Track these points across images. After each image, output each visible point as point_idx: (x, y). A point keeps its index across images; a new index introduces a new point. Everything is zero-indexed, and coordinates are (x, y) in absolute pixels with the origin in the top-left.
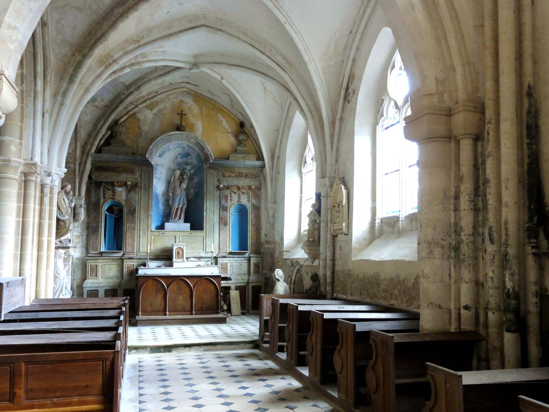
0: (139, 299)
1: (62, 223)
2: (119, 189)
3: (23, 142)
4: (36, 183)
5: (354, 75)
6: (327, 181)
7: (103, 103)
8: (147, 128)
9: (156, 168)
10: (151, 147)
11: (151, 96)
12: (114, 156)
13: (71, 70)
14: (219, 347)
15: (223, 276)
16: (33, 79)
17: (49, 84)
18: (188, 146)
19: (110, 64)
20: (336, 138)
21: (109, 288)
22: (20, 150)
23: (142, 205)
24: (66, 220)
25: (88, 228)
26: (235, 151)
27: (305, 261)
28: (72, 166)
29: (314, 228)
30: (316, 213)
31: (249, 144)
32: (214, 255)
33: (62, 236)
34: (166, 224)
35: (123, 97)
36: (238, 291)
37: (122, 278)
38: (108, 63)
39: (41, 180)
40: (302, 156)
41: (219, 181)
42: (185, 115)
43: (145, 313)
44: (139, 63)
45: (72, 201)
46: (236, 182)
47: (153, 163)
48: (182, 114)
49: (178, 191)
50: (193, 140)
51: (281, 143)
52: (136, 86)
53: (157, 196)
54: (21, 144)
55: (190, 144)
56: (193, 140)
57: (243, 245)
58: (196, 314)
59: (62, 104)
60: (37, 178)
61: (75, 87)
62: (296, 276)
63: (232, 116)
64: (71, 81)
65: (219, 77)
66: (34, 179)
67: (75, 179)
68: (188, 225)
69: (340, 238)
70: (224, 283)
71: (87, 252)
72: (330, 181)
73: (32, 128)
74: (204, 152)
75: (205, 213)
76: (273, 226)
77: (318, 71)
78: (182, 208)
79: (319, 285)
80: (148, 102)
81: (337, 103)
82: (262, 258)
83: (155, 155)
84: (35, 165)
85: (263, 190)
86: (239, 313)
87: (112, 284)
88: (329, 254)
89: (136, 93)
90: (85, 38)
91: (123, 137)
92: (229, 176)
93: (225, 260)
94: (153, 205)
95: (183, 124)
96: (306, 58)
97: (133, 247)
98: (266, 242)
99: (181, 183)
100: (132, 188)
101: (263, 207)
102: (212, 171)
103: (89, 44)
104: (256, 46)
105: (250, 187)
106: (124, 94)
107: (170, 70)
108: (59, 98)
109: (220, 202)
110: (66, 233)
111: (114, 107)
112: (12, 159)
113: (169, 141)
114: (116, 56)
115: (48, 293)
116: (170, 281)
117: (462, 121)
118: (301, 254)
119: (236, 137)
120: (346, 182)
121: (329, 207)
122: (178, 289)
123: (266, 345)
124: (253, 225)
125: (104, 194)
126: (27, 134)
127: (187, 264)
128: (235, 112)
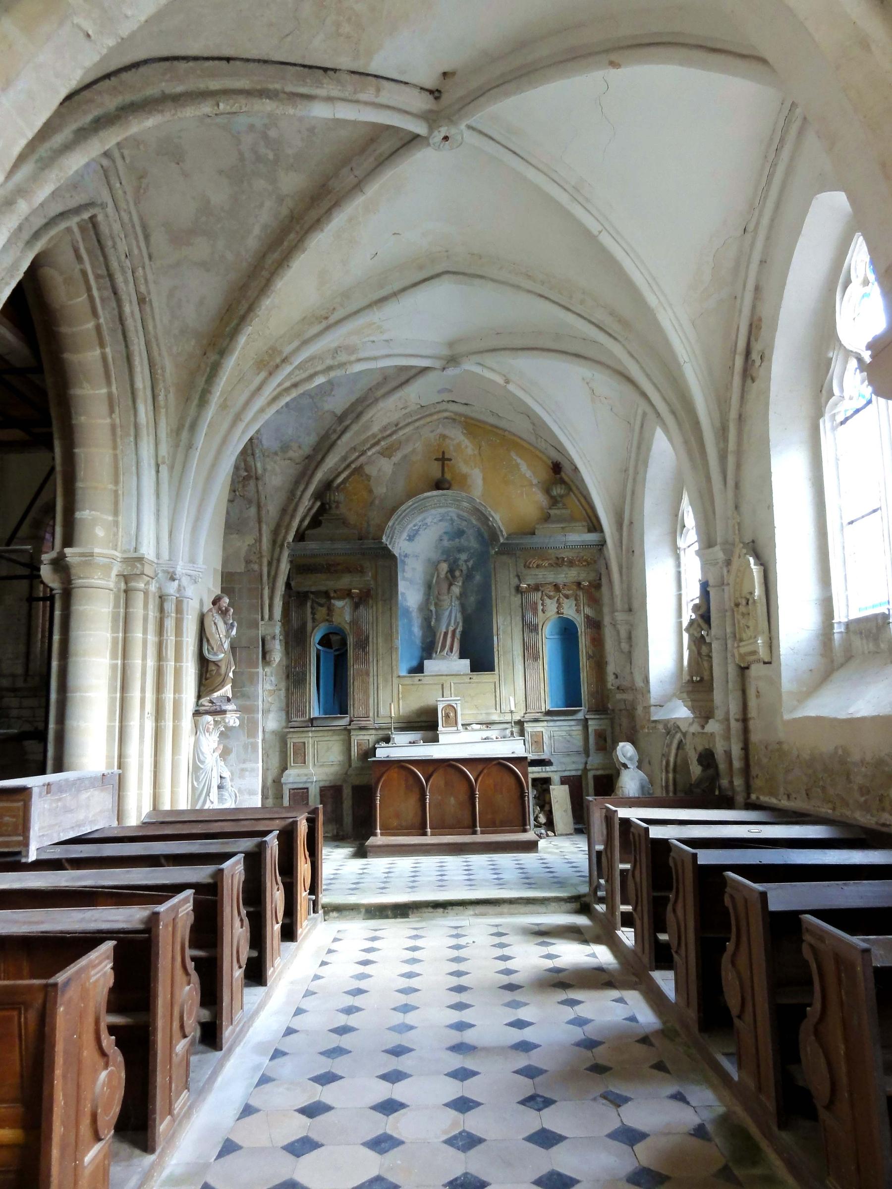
0: (376, 804)
1: (212, 667)
2: (339, 604)
3: (120, 518)
4: (146, 593)
5: (760, 320)
6: (718, 553)
7: (301, 452)
8: (384, 490)
9: (403, 562)
10: (390, 524)
11: (388, 432)
12: (328, 544)
13: (201, 382)
14: (505, 908)
15: (531, 756)
16: (130, 403)
17: (163, 411)
18: (459, 516)
19: (277, 367)
20: (731, 460)
21: (327, 784)
22: (116, 534)
23: (380, 629)
24: (220, 661)
25: (288, 677)
27: (691, 724)
28: (256, 567)
29: (699, 654)
30: (700, 621)
31: (572, 501)
32: (517, 717)
33: (214, 691)
34: (426, 662)
35: (334, 437)
36: (567, 787)
37: (350, 766)
38: (272, 364)
39: (160, 589)
40: (677, 516)
41: (518, 576)
42: (450, 460)
43: (388, 830)
44: (341, 365)
45: (232, 625)
47: (396, 552)
48: (443, 459)
49: (446, 600)
50: (465, 504)
51: (633, 493)
52: (354, 415)
53: (407, 611)
54: (116, 523)
55: (461, 513)
56: (465, 504)
57: (571, 696)
58: (483, 833)
59: (190, 446)
60: (147, 583)
61: (211, 411)
62: (676, 755)
63: (537, 452)
64: (203, 402)
65: (500, 380)
66: (142, 585)
67: (262, 589)
68: (467, 662)
69: (756, 671)
70: (535, 772)
71: (289, 720)
72: (724, 551)
73: (135, 492)
74: (488, 525)
75: (495, 638)
76: (629, 656)
77: (681, 325)
78: (454, 632)
79: (717, 775)
80: (383, 443)
81: (728, 387)
82: (612, 721)
83: (399, 538)
84: (140, 559)
85: (605, 589)
86: (572, 831)
87: (331, 778)
88: (734, 709)
89: (355, 428)
90: (222, 319)
91: (343, 510)
92: (538, 566)
93: (539, 727)
94: (400, 629)
95: (448, 476)
96: (652, 300)
97: (367, 706)
98: (618, 688)
99: (450, 585)
100: (362, 600)
101: (607, 620)
102: (504, 558)
103: (227, 329)
104: (552, 297)
105: (579, 584)
106: (335, 431)
107: (407, 376)
108: (185, 434)
109: (523, 617)
110: (222, 684)
111: (320, 457)
112: (97, 550)
113: (422, 509)
114: (287, 350)
116: (431, 769)
118: (681, 712)
119: (547, 491)
120: (761, 551)
121: (727, 607)
122: (446, 784)
123: (601, 908)
124: (589, 657)
125: (313, 614)
126: (127, 503)
127: (465, 736)
128: (542, 445)
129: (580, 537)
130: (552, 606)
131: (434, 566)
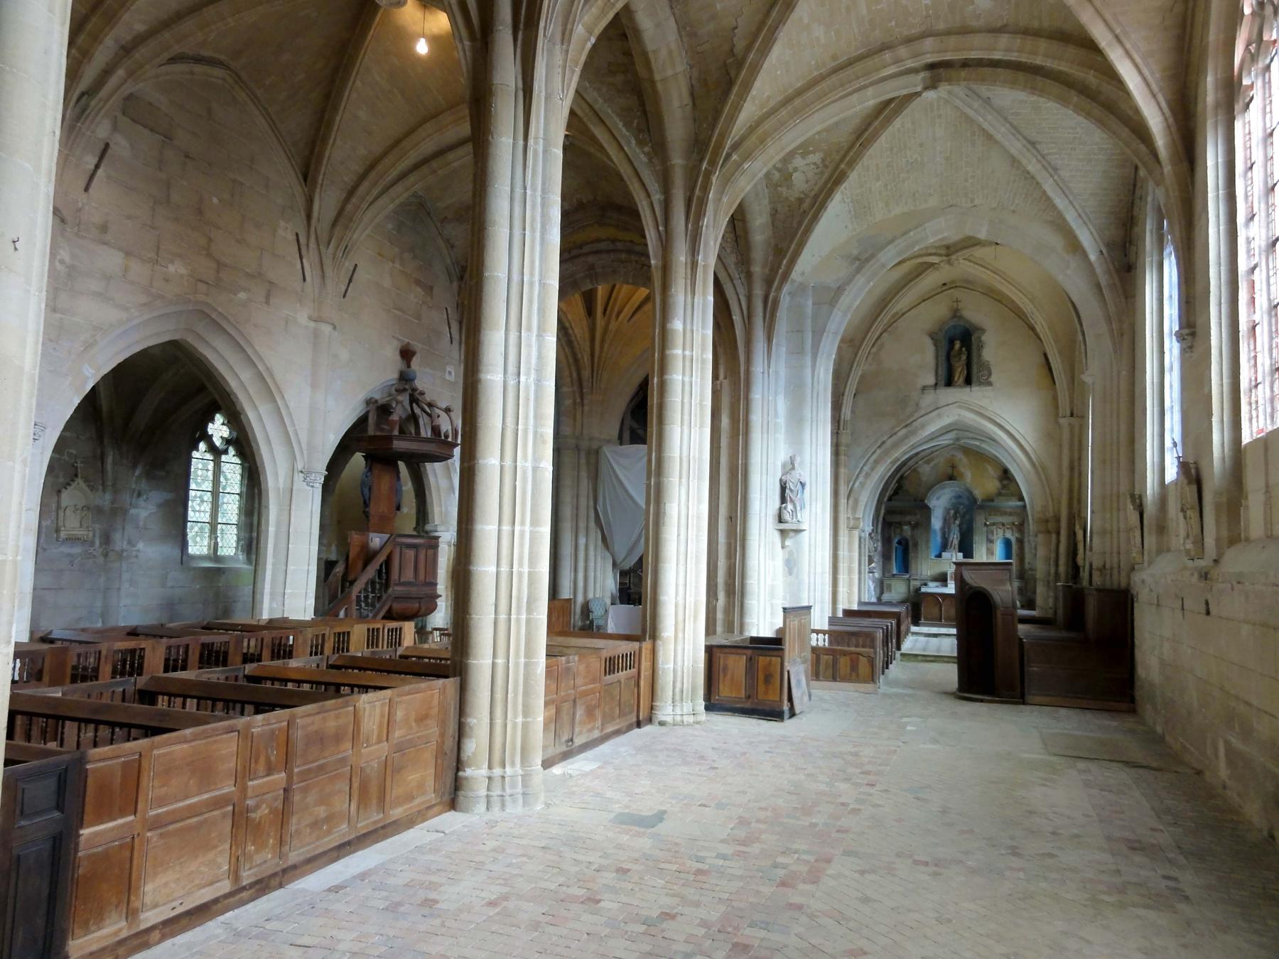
2: (906, 527)
26: (999, 494)
43: (926, 619)
48: (953, 467)
100: (915, 527)
117: (1051, 526)
119: (1001, 481)
130: (1000, 532)
131: (947, 511)
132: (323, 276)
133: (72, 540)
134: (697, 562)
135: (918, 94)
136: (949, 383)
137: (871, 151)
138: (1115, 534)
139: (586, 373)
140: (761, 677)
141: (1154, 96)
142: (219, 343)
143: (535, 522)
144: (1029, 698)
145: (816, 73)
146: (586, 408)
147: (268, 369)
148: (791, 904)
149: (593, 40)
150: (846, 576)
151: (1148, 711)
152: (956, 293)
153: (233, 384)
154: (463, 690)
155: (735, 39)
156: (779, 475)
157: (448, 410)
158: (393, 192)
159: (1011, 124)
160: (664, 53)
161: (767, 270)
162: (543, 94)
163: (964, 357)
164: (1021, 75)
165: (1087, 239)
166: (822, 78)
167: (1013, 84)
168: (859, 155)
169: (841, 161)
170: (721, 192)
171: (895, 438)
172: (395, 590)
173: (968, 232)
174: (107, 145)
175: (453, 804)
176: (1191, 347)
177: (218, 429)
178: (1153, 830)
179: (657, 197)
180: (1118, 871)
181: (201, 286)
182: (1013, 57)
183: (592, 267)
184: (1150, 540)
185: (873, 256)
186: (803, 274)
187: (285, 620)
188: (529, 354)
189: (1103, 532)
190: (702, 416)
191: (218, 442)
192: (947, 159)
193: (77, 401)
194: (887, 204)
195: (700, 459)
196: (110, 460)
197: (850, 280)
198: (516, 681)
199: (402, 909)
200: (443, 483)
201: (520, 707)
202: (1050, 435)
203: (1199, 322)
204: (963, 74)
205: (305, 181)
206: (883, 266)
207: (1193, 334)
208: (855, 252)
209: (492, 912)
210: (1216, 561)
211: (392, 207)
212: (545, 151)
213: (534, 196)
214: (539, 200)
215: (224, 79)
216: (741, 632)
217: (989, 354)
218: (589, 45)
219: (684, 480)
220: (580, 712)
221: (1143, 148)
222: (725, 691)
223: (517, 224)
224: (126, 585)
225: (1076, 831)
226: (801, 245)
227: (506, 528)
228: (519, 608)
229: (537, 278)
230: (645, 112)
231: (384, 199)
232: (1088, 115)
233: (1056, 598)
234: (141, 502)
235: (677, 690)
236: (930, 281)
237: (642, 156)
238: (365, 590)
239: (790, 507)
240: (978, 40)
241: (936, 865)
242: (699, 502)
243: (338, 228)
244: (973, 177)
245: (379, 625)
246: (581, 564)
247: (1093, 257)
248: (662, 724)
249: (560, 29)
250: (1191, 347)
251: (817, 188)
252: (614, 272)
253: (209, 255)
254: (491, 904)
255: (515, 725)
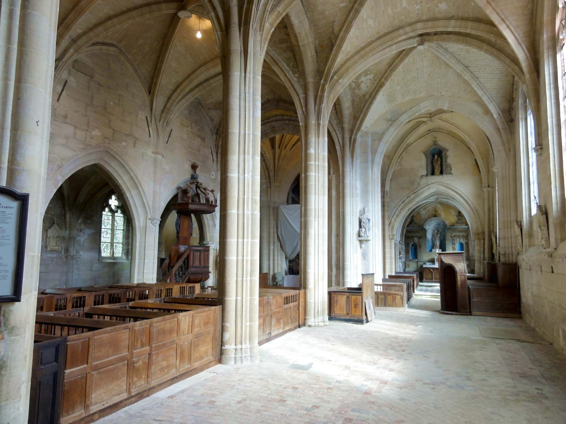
26: (457, 223)
46: (458, 234)
48: (436, 211)
100: (420, 238)
101: (470, 242)
115: (398, 271)
129: (464, 227)
130: (458, 240)
131: (434, 231)
132: (158, 134)
133: (52, 251)
134: (323, 255)
135: (415, 47)
136: (433, 174)
137: (395, 73)
138: (510, 239)
139: (272, 174)
140: (353, 305)
141: (520, 45)
142: (114, 164)
143: (253, 237)
144: (473, 313)
145: (370, 40)
146: (272, 189)
147: (135, 175)
148: (369, 402)
149: (273, 29)
150: (389, 261)
151: (527, 317)
152: (435, 134)
153: (120, 182)
154: (223, 310)
155: (334, 27)
156: (358, 216)
157: (212, 191)
158: (187, 97)
159: (457, 59)
160: (303, 34)
161: (350, 126)
162: (252, 53)
163: (439, 162)
164: (460, 37)
165: (493, 109)
166: (373, 42)
167: (457, 41)
168: (390, 74)
169: (382, 78)
170: (330, 93)
171: (409, 199)
172: (192, 270)
173: (439, 107)
174: (66, 82)
175: (220, 361)
176: (541, 154)
177: (113, 202)
178: (531, 369)
179: (302, 96)
180: (515, 386)
181: (107, 141)
182: (457, 30)
183: (273, 127)
184: (526, 241)
185: (397, 118)
186: (366, 127)
187: (144, 284)
188: (249, 165)
189: (504, 238)
190: (324, 191)
191: (113, 207)
192: (429, 75)
193: (55, 191)
194: (403, 96)
195: (323, 210)
196: (68, 216)
197: (387, 129)
198: (246, 307)
199: (200, 405)
200: (211, 223)
201: (248, 318)
202: (479, 196)
203: (544, 143)
204: (435, 38)
205: (150, 93)
206: (402, 123)
207: (541, 149)
208: (389, 117)
209: (239, 406)
210: (555, 249)
211: (186, 104)
212: (254, 78)
213: (249, 97)
214: (251, 98)
215: (114, 51)
216: (343, 285)
217: (450, 160)
218: (271, 32)
219: (317, 219)
220: (274, 321)
221: (516, 67)
222: (337, 311)
223: (242, 109)
224: (75, 271)
225: (496, 369)
226: (365, 115)
227: (240, 240)
228: (247, 275)
229: (251, 132)
230: (296, 59)
231: (183, 101)
232: (491, 54)
233: (484, 269)
234: (81, 234)
235: (316, 311)
236: (423, 129)
237: (295, 78)
238: (178, 270)
239: (363, 230)
240: (441, 23)
241: (434, 385)
242: (323, 228)
243: (164, 114)
244: (441, 83)
245: (185, 285)
246: (271, 258)
247: (495, 116)
248: (310, 326)
249: (259, 25)
250: (541, 154)
251: (371, 90)
252: (283, 129)
253: (110, 127)
254: (239, 402)
255: (246, 326)
